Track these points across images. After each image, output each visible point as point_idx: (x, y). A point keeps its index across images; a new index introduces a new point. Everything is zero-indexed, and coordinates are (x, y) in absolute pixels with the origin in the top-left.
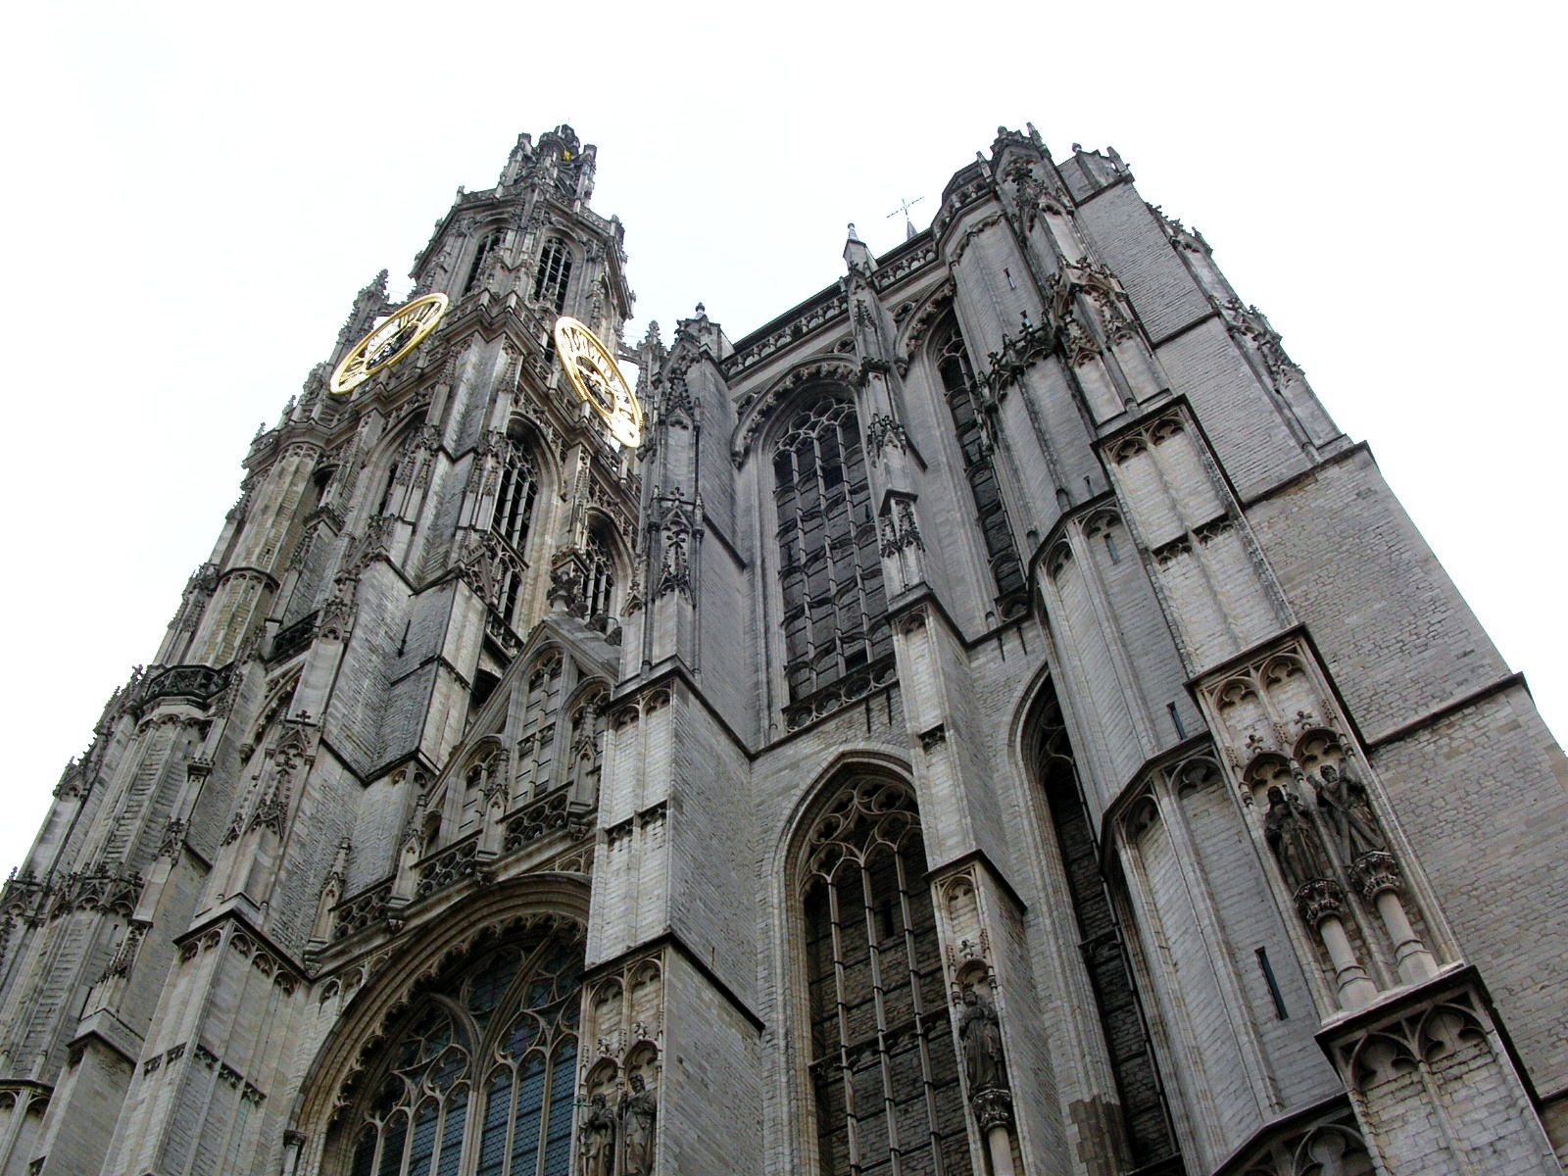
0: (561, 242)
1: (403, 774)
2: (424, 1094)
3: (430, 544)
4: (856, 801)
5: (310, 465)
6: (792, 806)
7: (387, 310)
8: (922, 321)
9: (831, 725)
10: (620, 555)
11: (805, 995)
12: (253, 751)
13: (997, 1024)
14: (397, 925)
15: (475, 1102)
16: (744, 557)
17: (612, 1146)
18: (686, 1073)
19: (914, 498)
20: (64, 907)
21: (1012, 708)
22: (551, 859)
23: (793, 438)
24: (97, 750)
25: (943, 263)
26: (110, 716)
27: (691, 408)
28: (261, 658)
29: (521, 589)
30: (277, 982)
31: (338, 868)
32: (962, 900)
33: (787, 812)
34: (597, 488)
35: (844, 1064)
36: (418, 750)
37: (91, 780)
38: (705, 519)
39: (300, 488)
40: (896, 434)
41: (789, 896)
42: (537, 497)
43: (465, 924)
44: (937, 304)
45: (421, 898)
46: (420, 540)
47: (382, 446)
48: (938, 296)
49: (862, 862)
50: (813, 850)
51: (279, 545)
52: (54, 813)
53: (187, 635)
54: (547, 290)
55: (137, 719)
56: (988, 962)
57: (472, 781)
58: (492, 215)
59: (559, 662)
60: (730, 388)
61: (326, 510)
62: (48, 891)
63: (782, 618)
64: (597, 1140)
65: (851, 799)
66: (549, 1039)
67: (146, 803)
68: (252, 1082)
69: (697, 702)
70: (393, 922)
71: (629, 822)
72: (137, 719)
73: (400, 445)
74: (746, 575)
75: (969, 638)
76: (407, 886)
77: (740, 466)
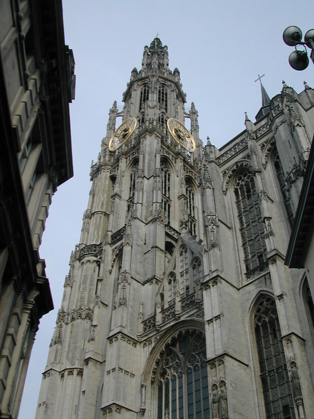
0: (163, 87)
1: (152, 282)
2: (172, 374)
3: (147, 208)
4: (265, 303)
5: (109, 175)
6: (250, 305)
7: (119, 115)
8: (268, 150)
10: (194, 186)
11: (257, 356)
12: (111, 271)
13: (299, 379)
15: (184, 377)
16: (229, 226)
17: (219, 406)
18: (233, 387)
19: (271, 218)
20: (73, 319)
21: (299, 282)
22: (193, 314)
23: (238, 183)
24: (72, 272)
25: (272, 131)
27: (211, 181)
29: (171, 208)
30: (133, 345)
31: (141, 311)
32: (289, 344)
33: (249, 307)
34: (186, 168)
35: (267, 375)
36: (155, 276)
37: (72, 281)
38: (219, 220)
40: (265, 196)
41: (251, 329)
44: (271, 144)
46: (144, 207)
48: (271, 142)
49: (267, 320)
50: (256, 316)
52: (65, 292)
53: (86, 233)
54: (162, 105)
55: (80, 261)
57: (170, 283)
58: (143, 82)
59: (186, 248)
60: (220, 168)
61: (116, 194)
62: (68, 314)
63: (242, 244)
64: (216, 405)
65: (263, 302)
66: (199, 361)
67: (87, 287)
68: (131, 372)
69: (224, 281)
70: (157, 328)
71: (212, 319)
74: (231, 230)
76: (159, 318)
77: (225, 194)
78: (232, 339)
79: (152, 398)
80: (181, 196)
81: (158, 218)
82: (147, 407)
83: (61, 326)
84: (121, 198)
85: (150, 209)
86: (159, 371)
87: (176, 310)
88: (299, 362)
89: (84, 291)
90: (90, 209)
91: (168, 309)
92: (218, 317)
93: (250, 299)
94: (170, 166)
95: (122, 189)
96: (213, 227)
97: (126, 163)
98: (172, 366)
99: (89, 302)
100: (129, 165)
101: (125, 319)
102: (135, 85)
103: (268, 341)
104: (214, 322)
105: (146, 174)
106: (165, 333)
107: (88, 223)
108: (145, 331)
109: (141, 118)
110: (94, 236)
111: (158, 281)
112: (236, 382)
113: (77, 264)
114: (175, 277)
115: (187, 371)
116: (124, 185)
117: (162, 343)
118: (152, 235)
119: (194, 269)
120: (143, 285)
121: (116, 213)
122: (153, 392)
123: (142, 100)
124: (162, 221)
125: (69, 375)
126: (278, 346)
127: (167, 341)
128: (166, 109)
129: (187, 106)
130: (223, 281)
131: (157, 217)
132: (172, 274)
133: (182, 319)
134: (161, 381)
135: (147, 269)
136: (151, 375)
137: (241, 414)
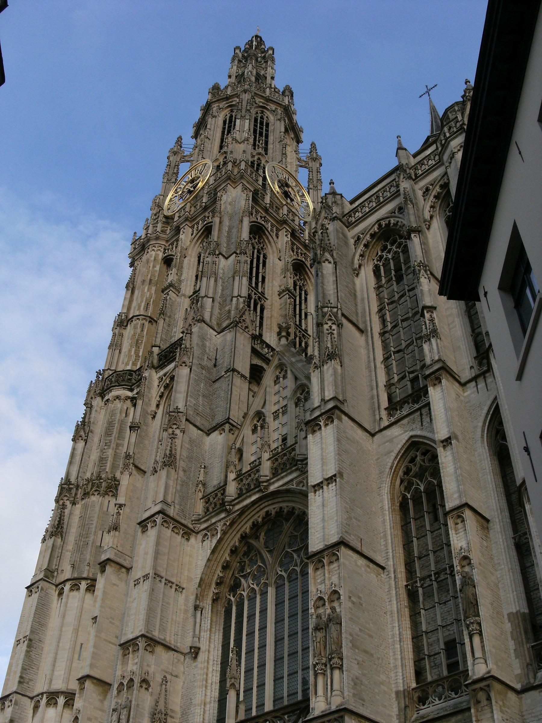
1: (223, 430)
2: (249, 586)
3: (222, 306)
4: (418, 458)
5: (161, 255)
6: (391, 461)
7: (184, 160)
8: (435, 197)
9: (405, 421)
10: (309, 278)
11: (401, 551)
12: (156, 413)
13: (475, 587)
14: (230, 509)
15: (271, 592)
16: (361, 326)
17: (326, 637)
18: (353, 603)
19: (435, 308)
20: (86, 494)
21: (482, 419)
22: (292, 480)
23: (381, 257)
24: (88, 415)
25: (443, 164)
26: (90, 397)
27: (332, 251)
28: (153, 367)
29: (265, 311)
30: (183, 536)
31: (201, 478)
32: (460, 525)
35: (419, 585)
36: (229, 418)
37: (87, 431)
38: (343, 315)
39: (158, 268)
40: (426, 271)
41: (393, 504)
42: (267, 260)
43: (258, 509)
44: (442, 187)
45: (240, 495)
46: (217, 305)
47: (192, 245)
48: (442, 182)
49: (422, 488)
50: (402, 481)
51: (152, 300)
52: (74, 449)
53: (118, 351)
54: (259, 142)
55: (103, 398)
56: (471, 557)
57: (254, 431)
58: (227, 103)
59: (286, 371)
60: (349, 231)
61: (171, 285)
62: (77, 487)
63: (382, 359)
64: (320, 635)
65: (416, 456)
66: (299, 564)
67: (113, 441)
68: (179, 584)
70: (228, 507)
71: (322, 482)
72: (103, 398)
73: (201, 243)
75: (463, 381)
76: (232, 489)
77: (357, 275)
78: (356, 519)
79: (213, 630)
80: (283, 291)
81: (240, 322)
82: (204, 646)
83: (64, 506)
85: (227, 308)
86: (228, 581)
87: (262, 474)
88: (475, 557)
89: (105, 447)
90: (125, 311)
91: (249, 474)
92: (330, 480)
93: (392, 451)
94: (267, 241)
95: (183, 278)
96: (331, 327)
97: (192, 235)
98: (250, 573)
99: (114, 467)
100: (196, 238)
101: (171, 490)
102: (215, 107)
103: (422, 526)
104: (325, 487)
105: (224, 250)
106: (240, 515)
107: (122, 335)
108: (206, 513)
109: (222, 163)
110: (130, 356)
111: (234, 429)
112: (361, 595)
113: (97, 402)
114: (264, 420)
115: (275, 582)
116: (185, 271)
117: (235, 532)
118: (227, 350)
119: (297, 405)
120: (208, 435)
121: (170, 317)
122: (214, 619)
124: (247, 327)
125: (71, 590)
126: (441, 535)
127: (243, 529)
128: (266, 150)
129: (305, 147)
131: (238, 320)
132: (260, 415)
133: (272, 488)
134: (230, 600)
135: (216, 408)
136: (213, 589)
137: (366, 652)
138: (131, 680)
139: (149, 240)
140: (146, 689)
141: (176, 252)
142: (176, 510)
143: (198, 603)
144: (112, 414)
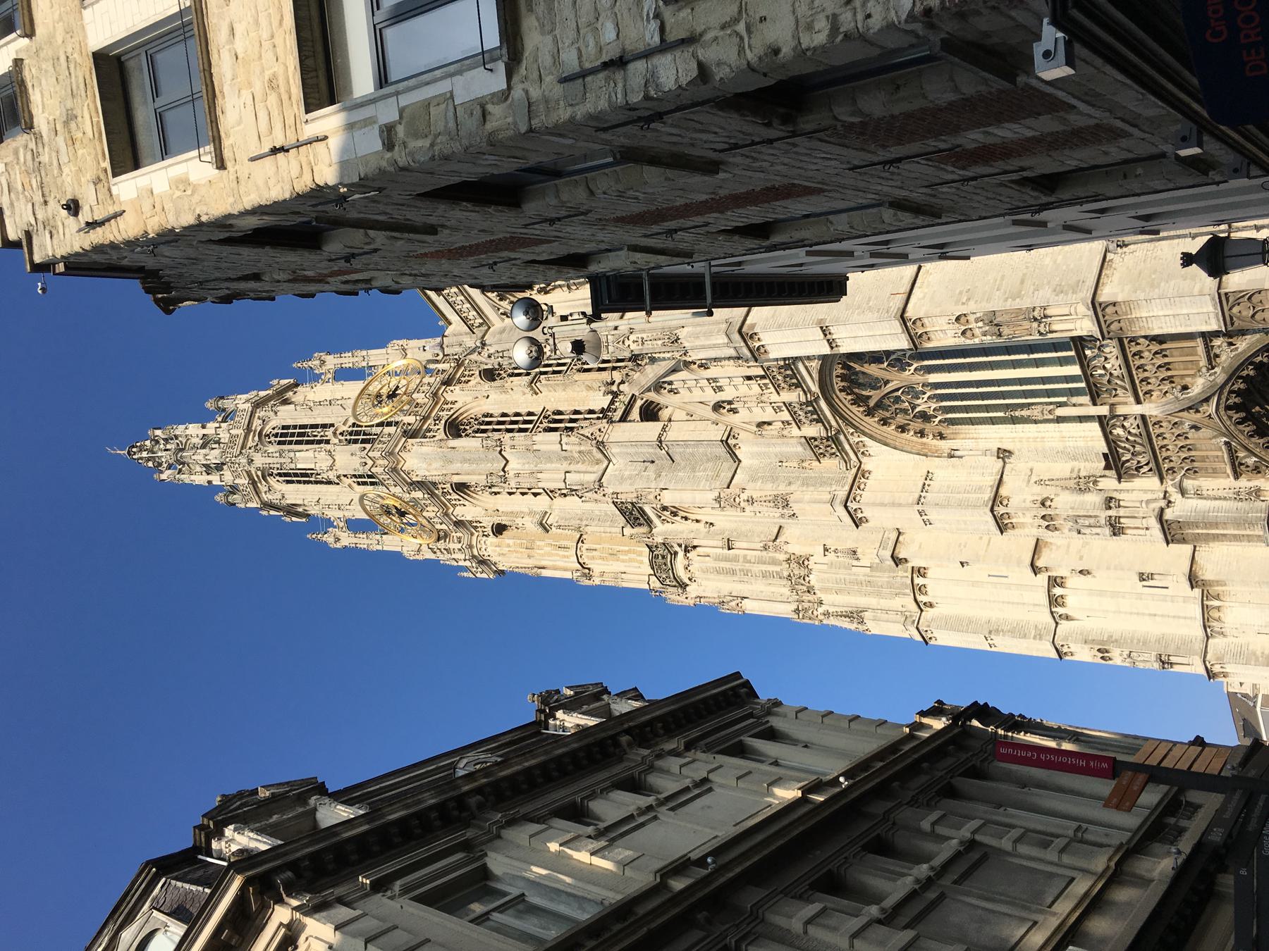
1: (735, 446)
5: (492, 539)
12: (707, 523)
36: (722, 441)
45: (819, 421)
57: (734, 411)
58: (260, 482)
70: (833, 433)
71: (828, 340)
78: (869, 301)
79: (975, 436)
80: (532, 389)
81: (595, 439)
84: (546, 513)
85: (576, 455)
86: (918, 425)
87: (797, 400)
89: (750, 575)
91: (793, 414)
92: (825, 331)
94: (464, 416)
95: (526, 510)
96: (634, 342)
98: (909, 403)
99: (774, 562)
101: (816, 496)
104: (834, 337)
110: (631, 560)
111: (732, 434)
112: (958, 291)
114: (723, 402)
116: (516, 509)
117: (863, 423)
118: (632, 450)
120: (740, 461)
121: (581, 520)
122: (962, 436)
123: (307, 479)
124: (600, 430)
127: (859, 415)
128: (324, 426)
130: (748, 322)
131: (595, 442)
132: (717, 407)
133: (815, 388)
134: (940, 421)
135: (706, 455)
136: (929, 441)
137: (1022, 282)
138: (1043, 517)
139: (474, 557)
140: (1051, 501)
141: (488, 522)
142: (838, 488)
143: (946, 455)
144: (705, 571)
